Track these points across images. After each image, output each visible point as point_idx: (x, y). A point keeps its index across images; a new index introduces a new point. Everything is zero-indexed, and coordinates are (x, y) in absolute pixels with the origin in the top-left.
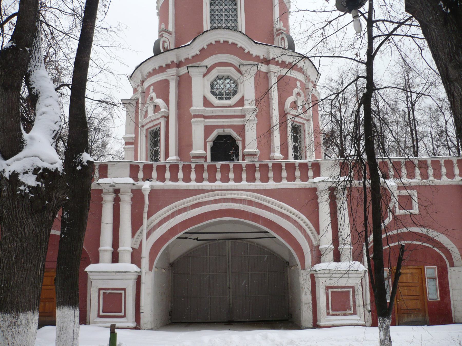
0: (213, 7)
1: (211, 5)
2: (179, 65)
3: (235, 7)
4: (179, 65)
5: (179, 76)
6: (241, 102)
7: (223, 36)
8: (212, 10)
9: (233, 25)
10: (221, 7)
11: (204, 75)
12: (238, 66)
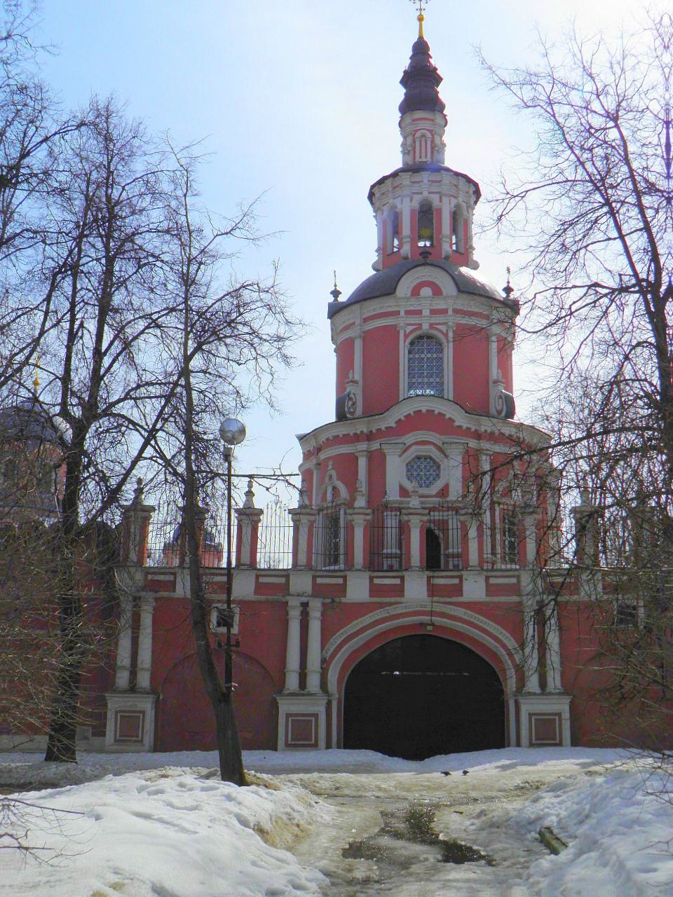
0: (411, 356)
1: (410, 353)
2: (370, 437)
3: (441, 355)
4: (370, 437)
5: (370, 452)
6: (444, 492)
7: (424, 406)
8: (410, 359)
9: (438, 380)
10: (423, 356)
11: (400, 456)
12: (441, 445)
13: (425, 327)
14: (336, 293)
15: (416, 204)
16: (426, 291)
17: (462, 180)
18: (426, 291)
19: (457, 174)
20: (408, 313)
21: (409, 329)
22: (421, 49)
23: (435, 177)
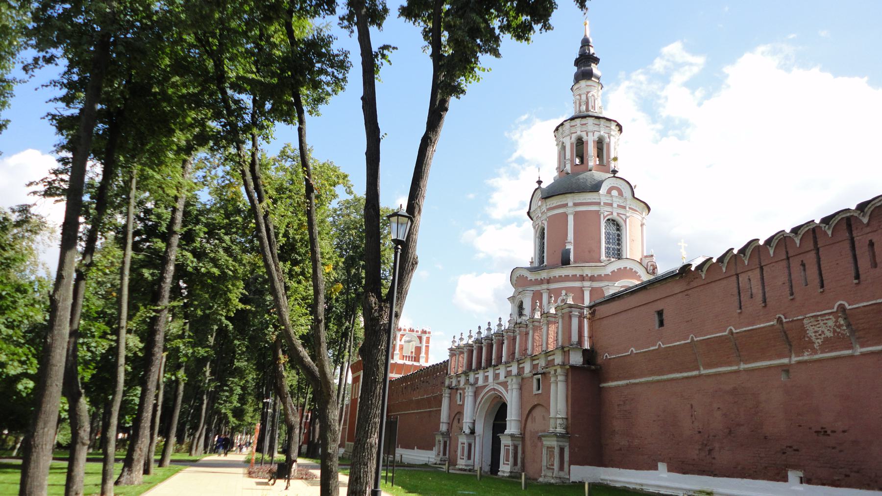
13: (615, 214)
14: (539, 182)
15: (596, 138)
16: (615, 193)
17: (618, 128)
18: (615, 193)
19: (618, 125)
20: (605, 203)
21: (606, 213)
22: (586, 43)
23: (608, 123)
